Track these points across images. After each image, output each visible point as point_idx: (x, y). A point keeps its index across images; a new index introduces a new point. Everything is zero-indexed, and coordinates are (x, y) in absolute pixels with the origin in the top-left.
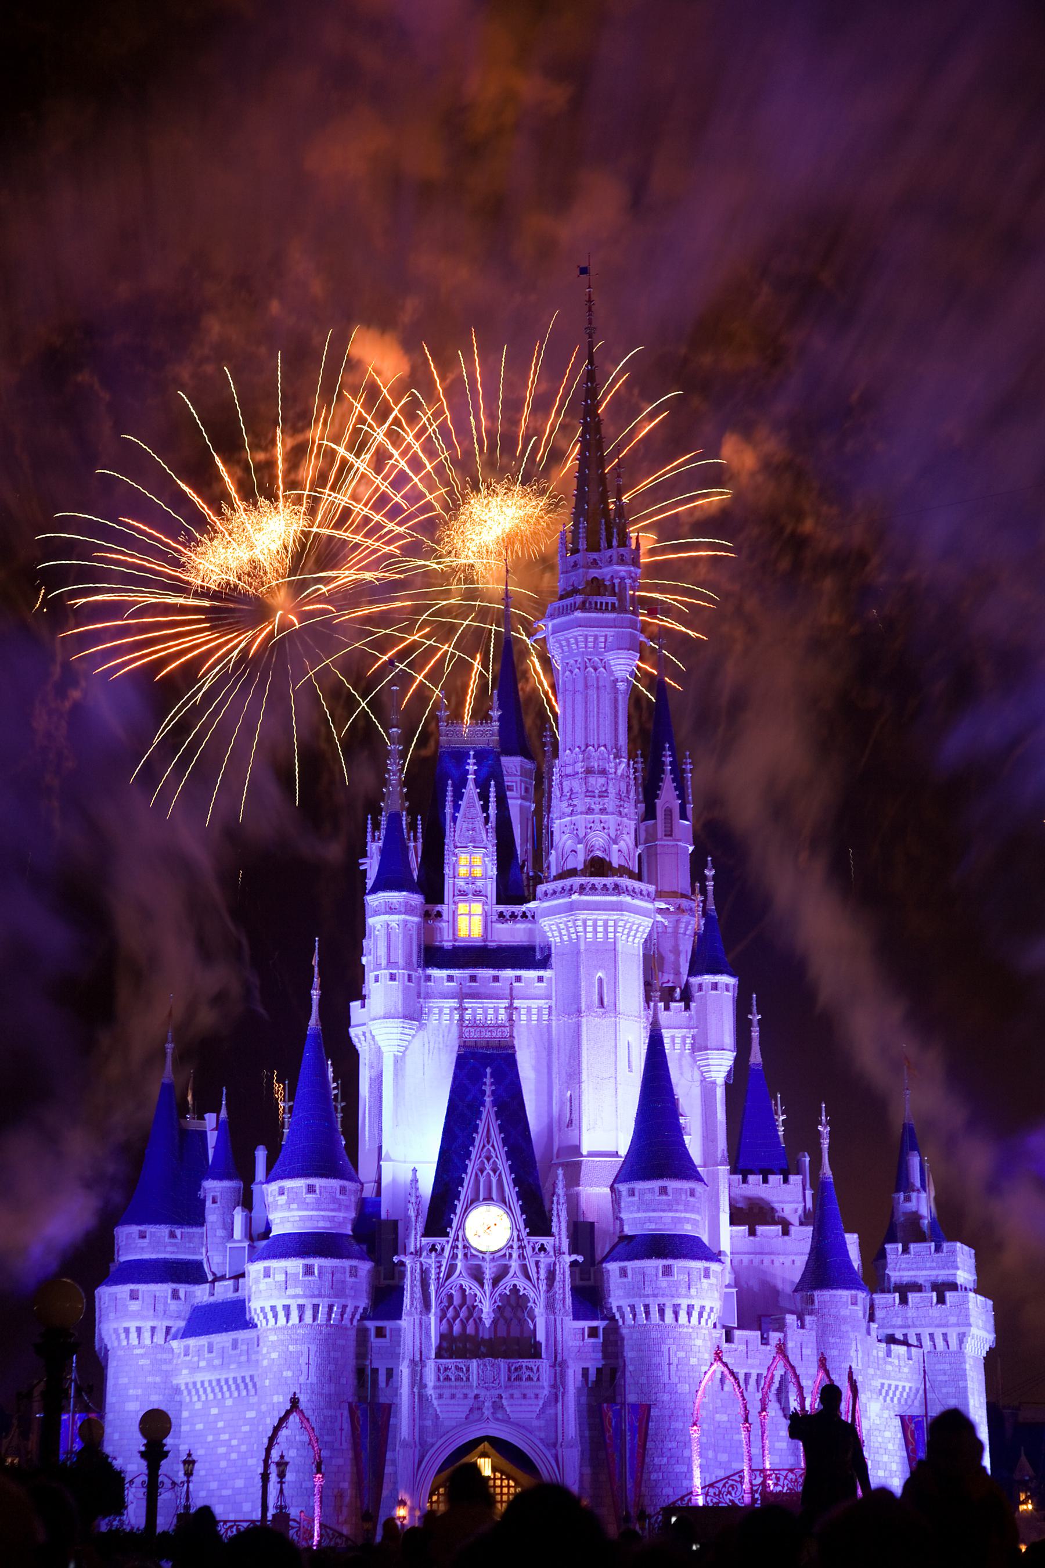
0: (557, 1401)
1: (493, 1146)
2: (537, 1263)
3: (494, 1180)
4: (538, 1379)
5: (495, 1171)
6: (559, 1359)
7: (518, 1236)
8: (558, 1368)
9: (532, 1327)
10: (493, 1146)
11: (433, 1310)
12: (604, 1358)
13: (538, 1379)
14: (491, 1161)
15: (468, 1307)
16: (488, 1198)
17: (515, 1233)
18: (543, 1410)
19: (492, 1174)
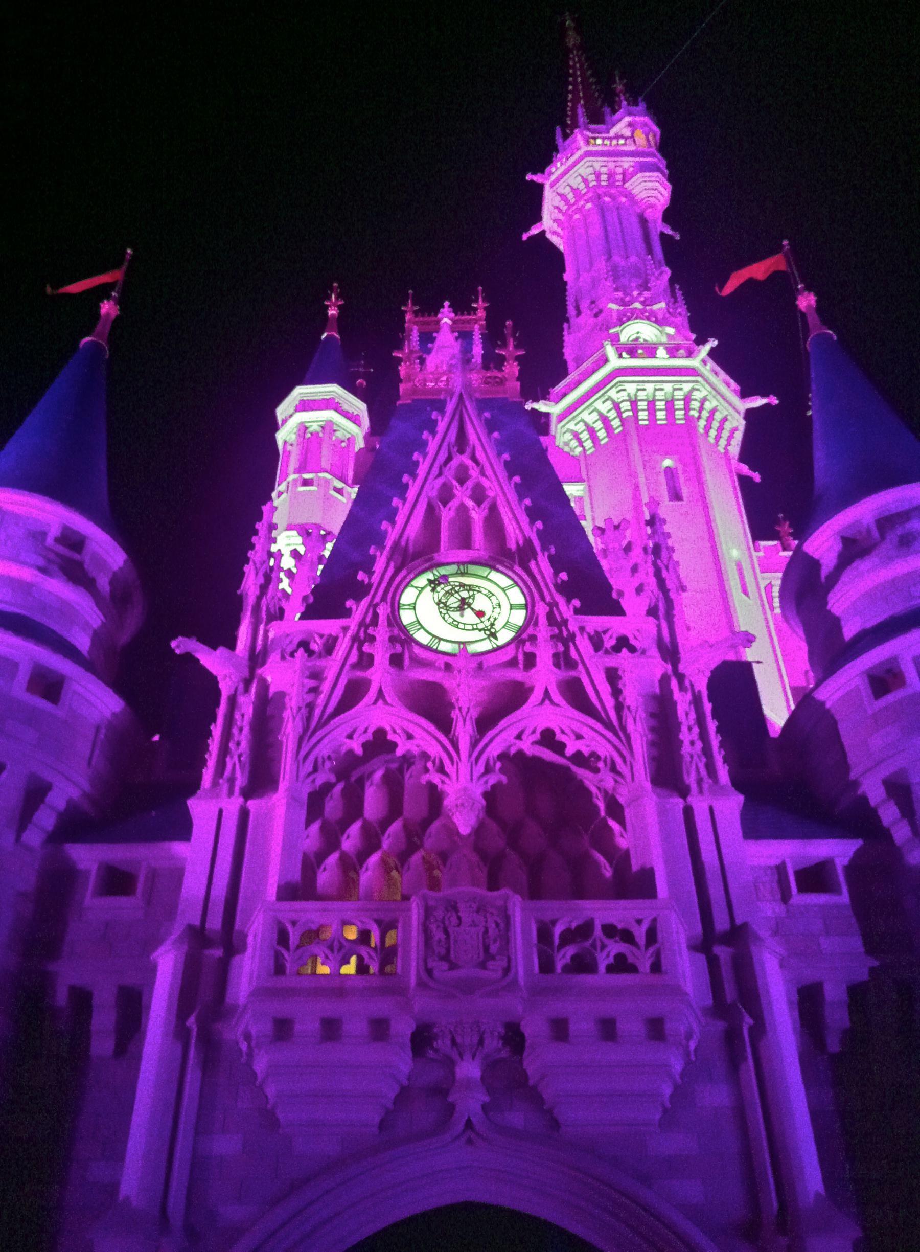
0: (734, 1062)
1: (474, 458)
2: (613, 676)
3: (477, 516)
4: (656, 967)
5: (479, 496)
6: (721, 924)
7: (550, 617)
8: (722, 952)
9: (608, 872)
10: (474, 458)
11: (283, 785)
12: (871, 949)
13: (656, 967)
14: (470, 484)
15: (405, 826)
16: (464, 540)
17: (542, 610)
18: (682, 1093)
19: (470, 503)
